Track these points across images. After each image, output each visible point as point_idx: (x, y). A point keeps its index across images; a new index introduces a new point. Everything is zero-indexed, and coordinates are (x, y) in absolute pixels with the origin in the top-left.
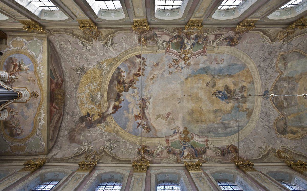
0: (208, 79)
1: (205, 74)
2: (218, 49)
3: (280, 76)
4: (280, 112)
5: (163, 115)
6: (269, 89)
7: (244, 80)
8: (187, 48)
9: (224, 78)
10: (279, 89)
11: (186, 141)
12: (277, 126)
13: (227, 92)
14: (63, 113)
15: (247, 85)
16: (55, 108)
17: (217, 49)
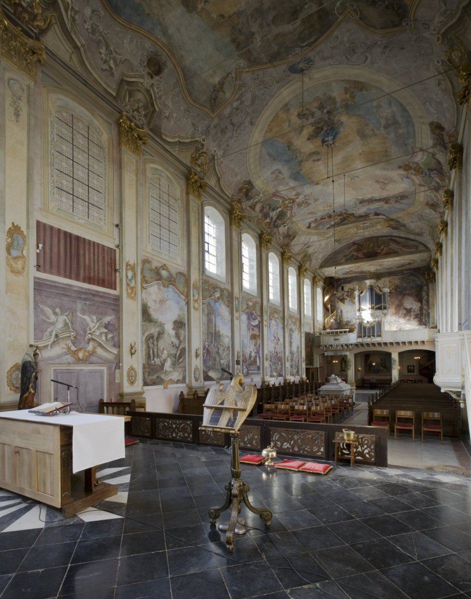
0: (307, 165)
1: (302, 172)
2: (263, 188)
3: (247, 70)
4: (339, 20)
5: (381, 186)
6: (284, 67)
7: (287, 124)
8: (280, 209)
9: (297, 149)
10: (276, 48)
11: (420, 170)
12: (382, 28)
13: (321, 131)
14: (389, 238)
15: (294, 112)
16: (383, 250)
17: (263, 190)
